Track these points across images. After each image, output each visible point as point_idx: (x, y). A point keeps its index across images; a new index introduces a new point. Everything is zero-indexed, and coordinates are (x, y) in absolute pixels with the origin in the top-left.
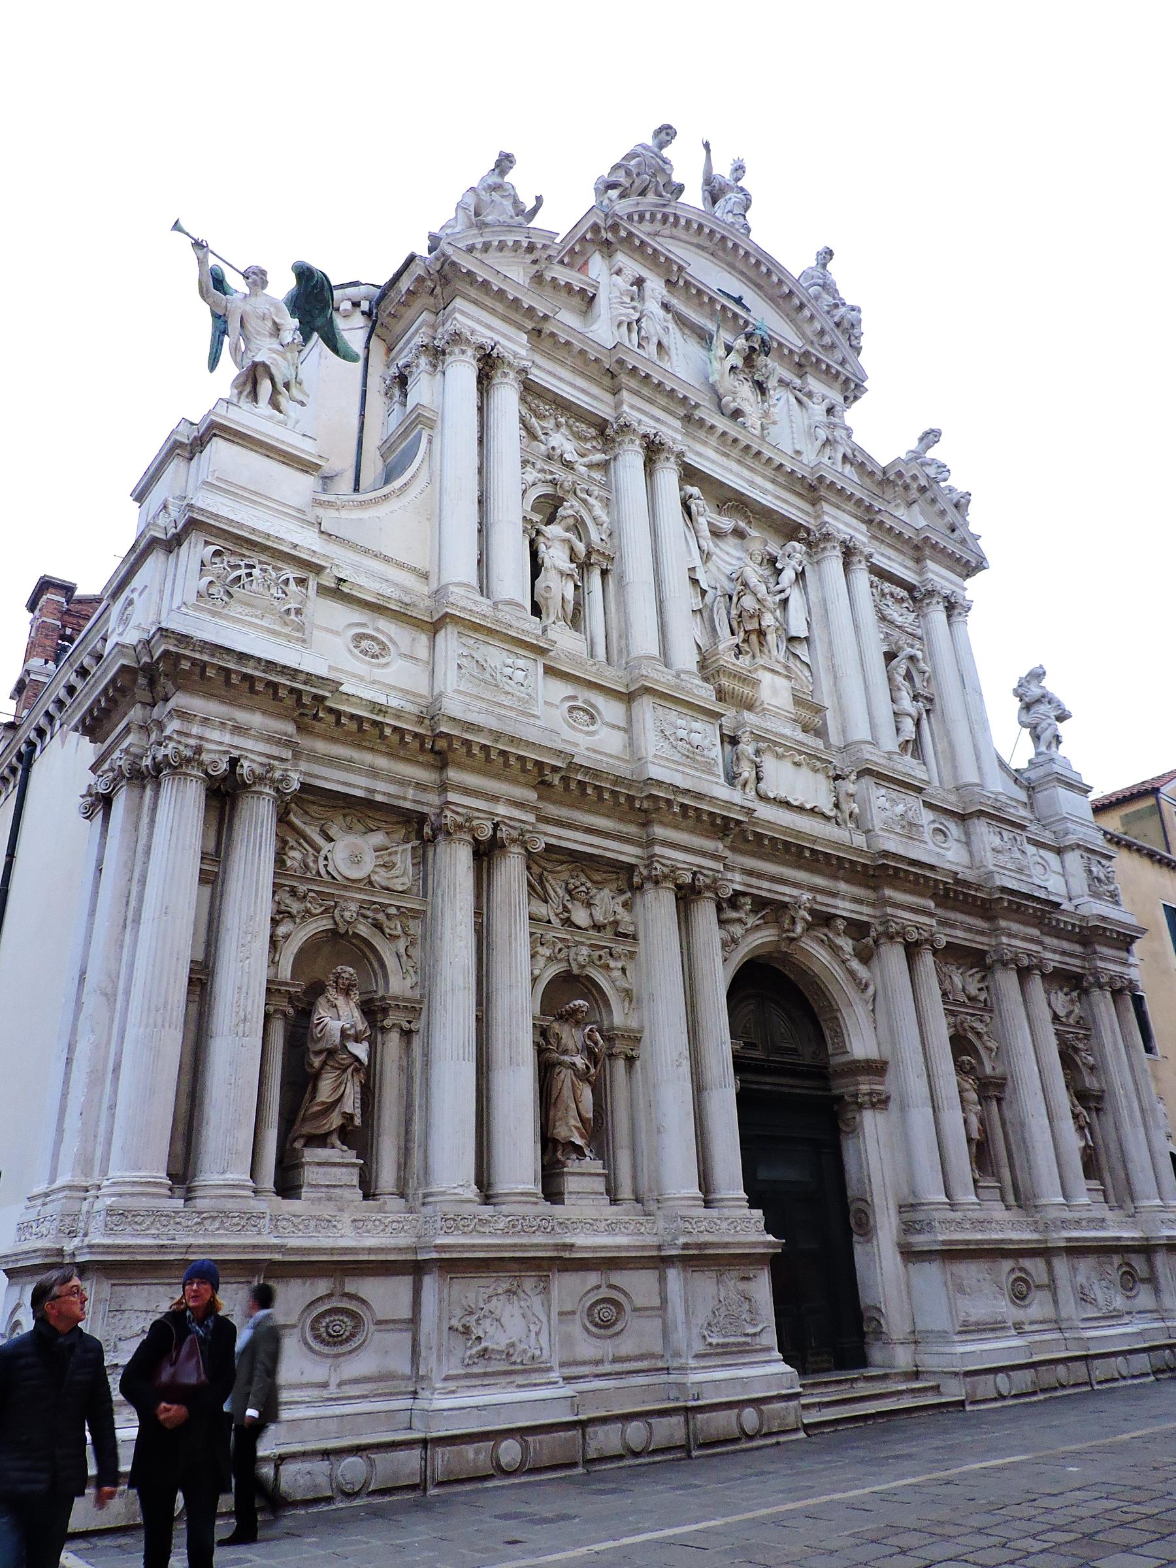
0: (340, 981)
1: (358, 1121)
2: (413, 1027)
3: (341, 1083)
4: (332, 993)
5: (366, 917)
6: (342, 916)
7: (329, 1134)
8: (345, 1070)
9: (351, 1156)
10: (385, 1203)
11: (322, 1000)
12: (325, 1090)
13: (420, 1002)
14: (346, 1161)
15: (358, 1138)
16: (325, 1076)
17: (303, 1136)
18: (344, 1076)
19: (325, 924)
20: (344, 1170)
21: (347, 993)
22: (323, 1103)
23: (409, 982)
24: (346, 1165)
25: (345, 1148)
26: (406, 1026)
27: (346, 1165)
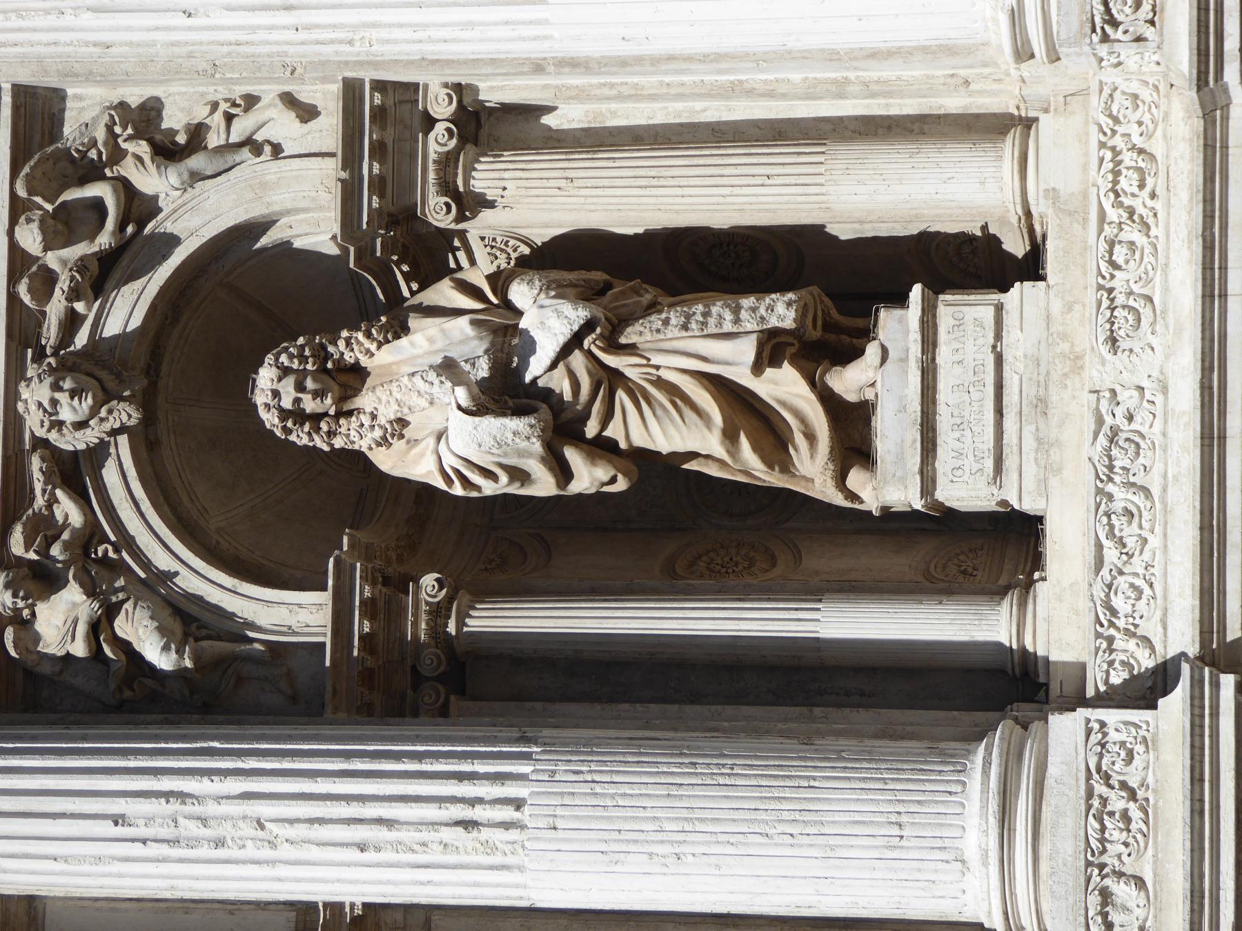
0: (310, 405)
1: (781, 312)
2: (442, 108)
3: (660, 383)
4: (356, 436)
5: (72, 321)
6: (81, 425)
7: (829, 399)
8: (615, 378)
9: (898, 327)
10: (1052, 194)
11: (387, 461)
12: (691, 435)
13: (352, 91)
14: (915, 350)
15: (841, 288)
16: (640, 439)
17: (841, 479)
18: (630, 373)
19: (120, 477)
20: (944, 355)
21: (352, 378)
22: (730, 436)
23: (280, 126)
24: (929, 341)
25: (872, 350)
26: (438, 141)
27: (929, 341)
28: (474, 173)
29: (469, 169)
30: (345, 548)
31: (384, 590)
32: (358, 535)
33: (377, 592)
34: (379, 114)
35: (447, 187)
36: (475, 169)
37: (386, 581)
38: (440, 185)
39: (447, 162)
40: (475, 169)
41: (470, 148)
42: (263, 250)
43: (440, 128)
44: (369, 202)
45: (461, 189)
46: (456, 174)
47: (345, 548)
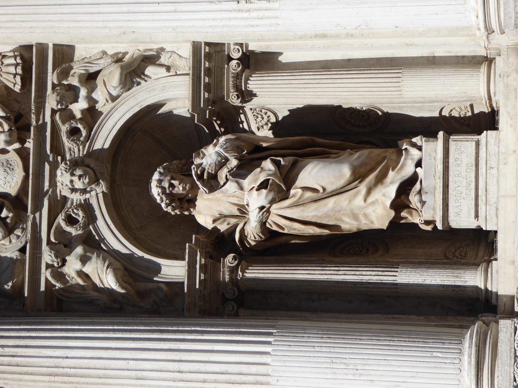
13: (196, 47)
28: (249, 82)
29: (247, 79)
30: (193, 243)
31: (210, 261)
32: (198, 236)
33: (207, 261)
34: (208, 56)
35: (238, 88)
36: (250, 80)
37: (211, 257)
38: (234, 87)
39: (238, 77)
40: (250, 80)
41: (247, 71)
42: (159, 114)
43: (234, 63)
44: (204, 95)
45: (243, 89)
46: (241, 82)
47: (193, 243)
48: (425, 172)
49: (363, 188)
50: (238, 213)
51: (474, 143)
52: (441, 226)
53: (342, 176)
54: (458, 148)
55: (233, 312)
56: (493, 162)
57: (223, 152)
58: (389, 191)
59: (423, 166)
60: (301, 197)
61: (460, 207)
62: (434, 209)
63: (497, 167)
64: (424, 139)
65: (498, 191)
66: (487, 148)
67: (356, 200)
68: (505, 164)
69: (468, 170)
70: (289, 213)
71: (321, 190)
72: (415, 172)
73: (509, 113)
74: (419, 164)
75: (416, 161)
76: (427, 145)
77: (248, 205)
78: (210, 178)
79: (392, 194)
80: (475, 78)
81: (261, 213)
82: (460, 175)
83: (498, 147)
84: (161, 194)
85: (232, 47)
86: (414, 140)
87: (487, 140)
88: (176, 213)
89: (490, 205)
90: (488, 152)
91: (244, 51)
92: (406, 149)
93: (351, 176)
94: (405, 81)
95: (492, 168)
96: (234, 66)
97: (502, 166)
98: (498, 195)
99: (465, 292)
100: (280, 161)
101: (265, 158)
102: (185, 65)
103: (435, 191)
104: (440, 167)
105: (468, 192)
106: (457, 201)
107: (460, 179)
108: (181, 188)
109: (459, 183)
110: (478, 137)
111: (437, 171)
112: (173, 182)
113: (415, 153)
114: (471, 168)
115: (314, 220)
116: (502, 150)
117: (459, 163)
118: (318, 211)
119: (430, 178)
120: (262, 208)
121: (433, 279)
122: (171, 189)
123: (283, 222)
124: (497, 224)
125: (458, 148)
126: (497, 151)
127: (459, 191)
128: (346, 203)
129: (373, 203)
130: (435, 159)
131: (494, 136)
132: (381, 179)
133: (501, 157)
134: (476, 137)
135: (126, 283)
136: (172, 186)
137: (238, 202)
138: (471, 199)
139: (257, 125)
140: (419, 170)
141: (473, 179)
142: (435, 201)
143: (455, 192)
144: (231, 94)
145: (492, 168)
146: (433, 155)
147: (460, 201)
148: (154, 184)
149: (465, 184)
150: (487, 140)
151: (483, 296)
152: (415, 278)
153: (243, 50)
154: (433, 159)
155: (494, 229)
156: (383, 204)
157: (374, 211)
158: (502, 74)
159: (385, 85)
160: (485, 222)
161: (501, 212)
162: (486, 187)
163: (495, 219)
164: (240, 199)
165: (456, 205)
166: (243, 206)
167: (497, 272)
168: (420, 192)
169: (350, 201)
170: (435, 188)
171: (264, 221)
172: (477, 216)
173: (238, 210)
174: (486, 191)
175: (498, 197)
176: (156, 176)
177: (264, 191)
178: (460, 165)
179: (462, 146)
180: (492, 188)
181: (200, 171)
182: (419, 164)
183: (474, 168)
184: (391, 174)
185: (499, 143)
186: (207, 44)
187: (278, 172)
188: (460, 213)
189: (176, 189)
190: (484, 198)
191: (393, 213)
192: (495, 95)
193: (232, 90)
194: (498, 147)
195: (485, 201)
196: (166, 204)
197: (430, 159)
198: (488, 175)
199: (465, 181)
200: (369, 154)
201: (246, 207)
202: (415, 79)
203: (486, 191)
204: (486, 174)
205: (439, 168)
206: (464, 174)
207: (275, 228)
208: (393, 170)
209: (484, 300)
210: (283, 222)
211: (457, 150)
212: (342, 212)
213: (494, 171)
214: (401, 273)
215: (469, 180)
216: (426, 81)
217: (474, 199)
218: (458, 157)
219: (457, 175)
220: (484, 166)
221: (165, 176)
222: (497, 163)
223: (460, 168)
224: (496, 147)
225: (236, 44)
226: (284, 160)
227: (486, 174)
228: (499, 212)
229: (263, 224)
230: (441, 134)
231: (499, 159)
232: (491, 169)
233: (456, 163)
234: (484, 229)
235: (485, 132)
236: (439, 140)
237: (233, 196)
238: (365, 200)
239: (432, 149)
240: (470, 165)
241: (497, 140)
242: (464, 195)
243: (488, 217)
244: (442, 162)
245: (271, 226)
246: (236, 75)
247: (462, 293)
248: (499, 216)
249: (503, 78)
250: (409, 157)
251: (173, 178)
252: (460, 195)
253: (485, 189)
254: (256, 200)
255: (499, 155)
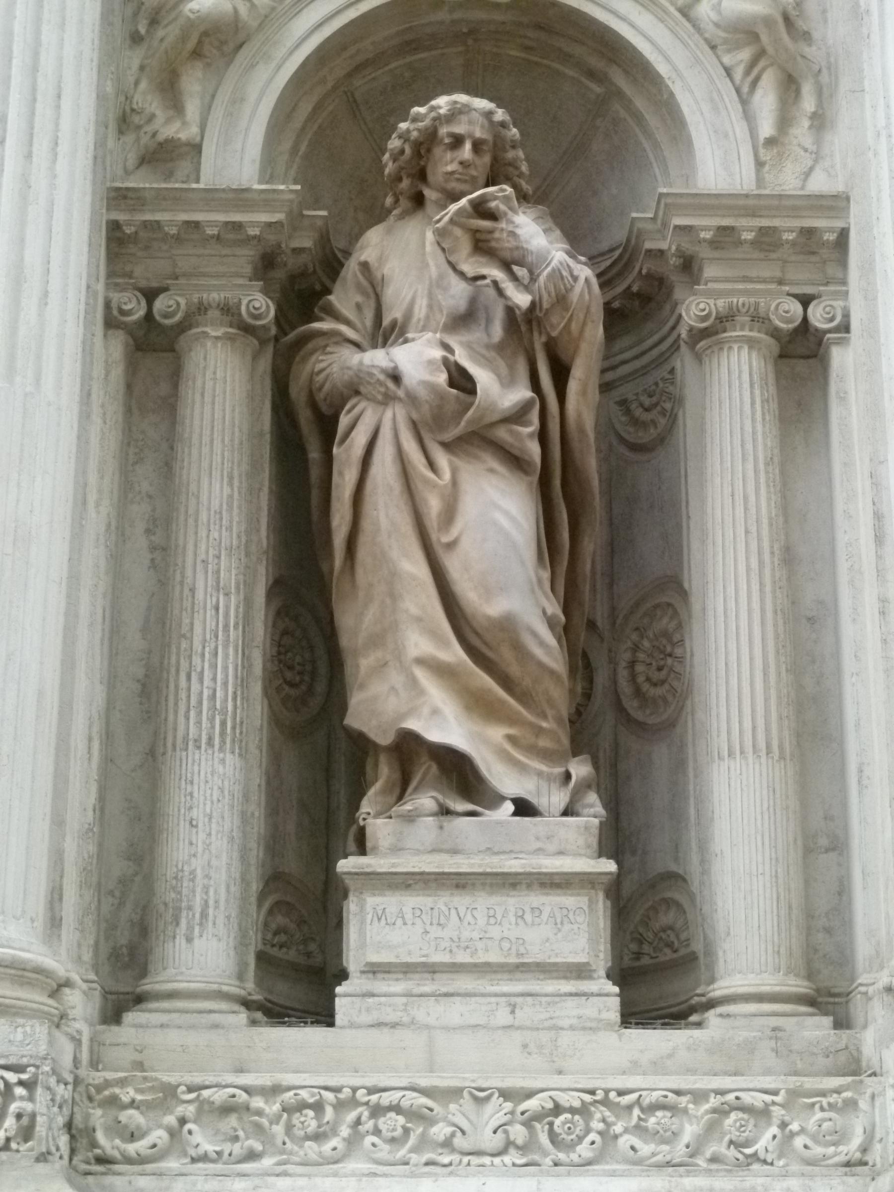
13: (837, 203)
29: (751, 343)
48: (499, 823)
49: (454, 653)
50: (386, 322)
51: (582, 958)
52: (345, 870)
53: (488, 593)
54: (571, 914)
55: (115, 312)
56: (528, 1013)
57: (549, 269)
58: (446, 724)
59: (518, 818)
60: (426, 481)
61: (399, 922)
62: (396, 850)
63: (517, 1023)
64: (596, 821)
65: (446, 1029)
66: (571, 995)
67: (424, 635)
68: (525, 1046)
69: (506, 945)
70: (384, 454)
71: (445, 539)
72: (502, 798)
73: (670, 1056)
74: (524, 808)
75: (534, 801)
76: (578, 827)
77: (406, 341)
78: (478, 235)
79: (434, 735)
80: (770, 959)
81: (382, 377)
82: (492, 921)
83: (572, 1028)
84: (433, 114)
85: (839, 304)
86: (592, 797)
87: (592, 995)
88: (386, 165)
89: (406, 1005)
90: (557, 999)
91: (828, 335)
92: (568, 776)
93: (489, 618)
94: (757, 766)
95: (513, 1012)
96: (787, 308)
97: (517, 1036)
98: (434, 1028)
99: (162, 938)
100: (526, 424)
101: (535, 384)
102: (787, 180)
103: (447, 851)
104: (513, 865)
105: (444, 944)
106: (418, 913)
107: (482, 921)
108: (449, 168)
109: (469, 918)
110: (602, 973)
111: (502, 857)
112: (468, 146)
113: (559, 798)
114: (514, 951)
115: (366, 525)
116: (566, 1039)
117: (528, 917)
118: (389, 536)
119: (483, 839)
120: (396, 377)
121: (200, 849)
122: (447, 141)
123: (360, 438)
124: (352, 1025)
125: (571, 915)
126: (561, 1023)
127: (448, 918)
128: (414, 610)
129: (414, 682)
130: (539, 851)
131: (605, 1015)
132: (479, 706)
133: (545, 1037)
134: (602, 962)
135: (200, 42)
136: (457, 141)
137: (414, 320)
138: (424, 952)
139: (631, 397)
140: (509, 807)
141: (482, 958)
142: (418, 852)
143: (444, 908)
144: (711, 302)
145: (513, 1012)
146: (551, 847)
147: (418, 921)
148: (462, 98)
149: (466, 934)
150: (592, 995)
151: (147, 988)
152: (202, 798)
153: (829, 331)
154: (539, 845)
155: (339, 1019)
156: (411, 712)
157: (393, 688)
158: (780, 1034)
159: (747, 710)
160: (358, 991)
161: (384, 1037)
162: (459, 995)
163: (365, 1019)
164: (422, 323)
165: (407, 910)
166: (403, 332)
167: (216, 1026)
168: (445, 812)
169: (419, 620)
170: (455, 852)
171: (362, 389)
172: (374, 970)
173: (394, 324)
174: (446, 995)
175: (428, 1027)
176: (482, 104)
177: (442, 378)
178: (519, 920)
179: (575, 926)
180: (456, 1012)
181: (497, 206)
182: (524, 808)
183: (513, 960)
184: (498, 733)
185: (584, 1029)
186: (844, 234)
187: (496, 417)
188: (383, 921)
189: (449, 155)
190: (427, 989)
191: (385, 739)
192: (721, 1015)
193: (721, 303)
194: (572, 1028)
195: (417, 990)
196: (408, 131)
197: (538, 839)
198: (493, 999)
199: (476, 935)
200: (552, 673)
201: (401, 340)
202: (765, 792)
203: (446, 995)
204: (496, 995)
205: (514, 862)
206: (495, 932)
207: (344, 421)
208: (510, 738)
209: (139, 990)
210: (360, 438)
211: (565, 912)
212: (388, 601)
213: (503, 1017)
214: (216, 760)
215: (480, 945)
216: (759, 822)
217: (423, 960)
218: (545, 916)
219: (492, 912)
220: (519, 987)
221: (482, 127)
222: (528, 1023)
223: (513, 920)
224: (574, 1021)
225: (846, 316)
226: (531, 435)
227: (496, 995)
228: (386, 1030)
229: (354, 389)
230: (610, 866)
231: (538, 1029)
232: (509, 1009)
233: (527, 910)
234: (338, 990)
235: (617, 989)
236: (592, 862)
237: (430, 307)
238: (421, 661)
239: (570, 843)
240: (522, 950)
241: (593, 1025)
242: (435, 932)
243: (371, 1000)
244: (528, 869)
245: (349, 411)
246: (762, 315)
247: (161, 927)
248: (374, 1032)
249: (771, 1038)
250: (544, 785)
251: (477, 146)
252: (435, 922)
253: (451, 990)
254: (417, 359)
255: (550, 1028)
